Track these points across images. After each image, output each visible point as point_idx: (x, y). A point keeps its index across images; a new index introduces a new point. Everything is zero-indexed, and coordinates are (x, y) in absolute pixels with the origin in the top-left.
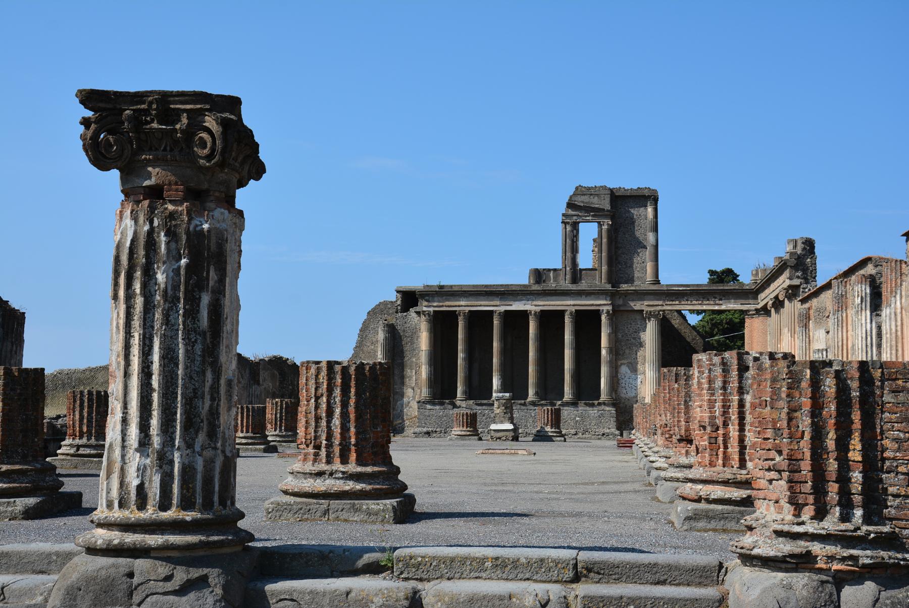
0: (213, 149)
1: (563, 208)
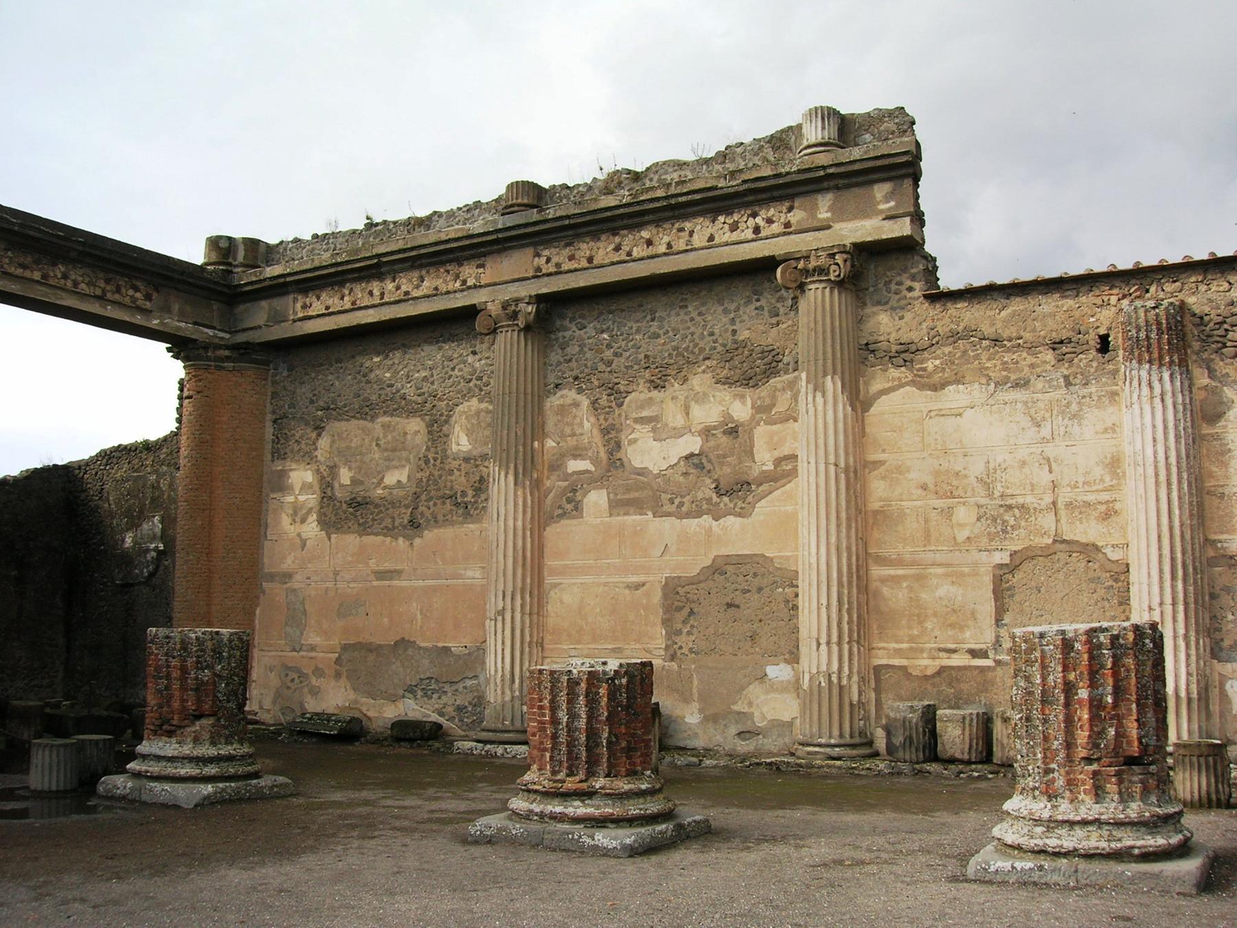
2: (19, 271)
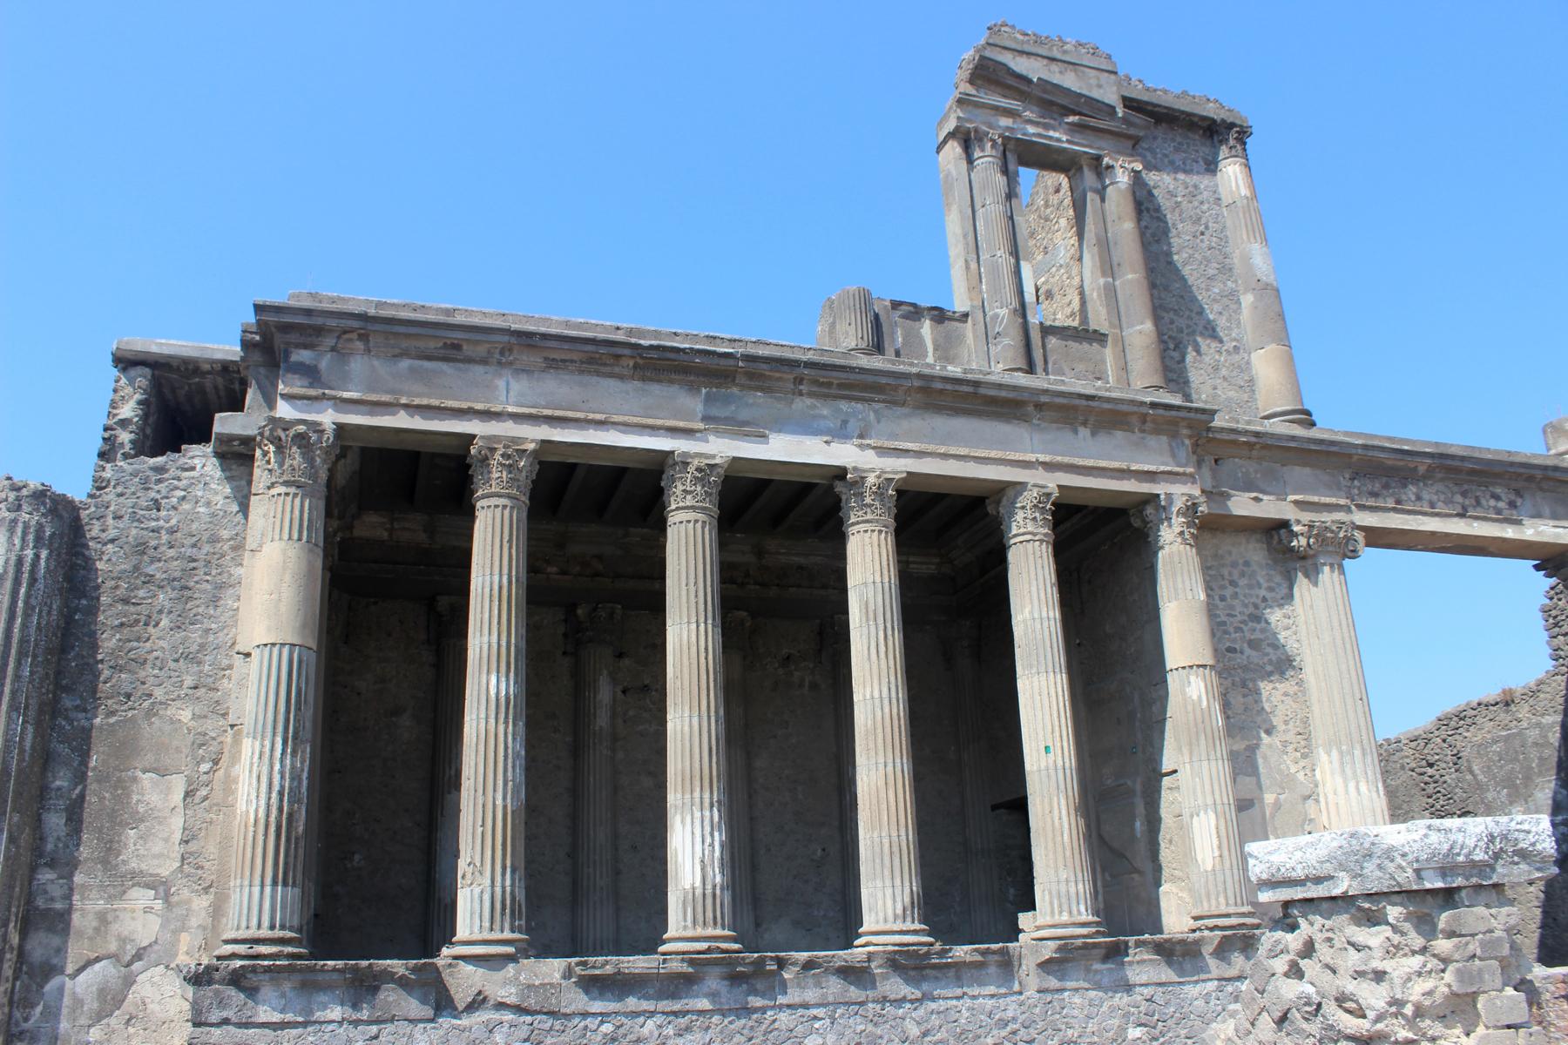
1: (957, 81)
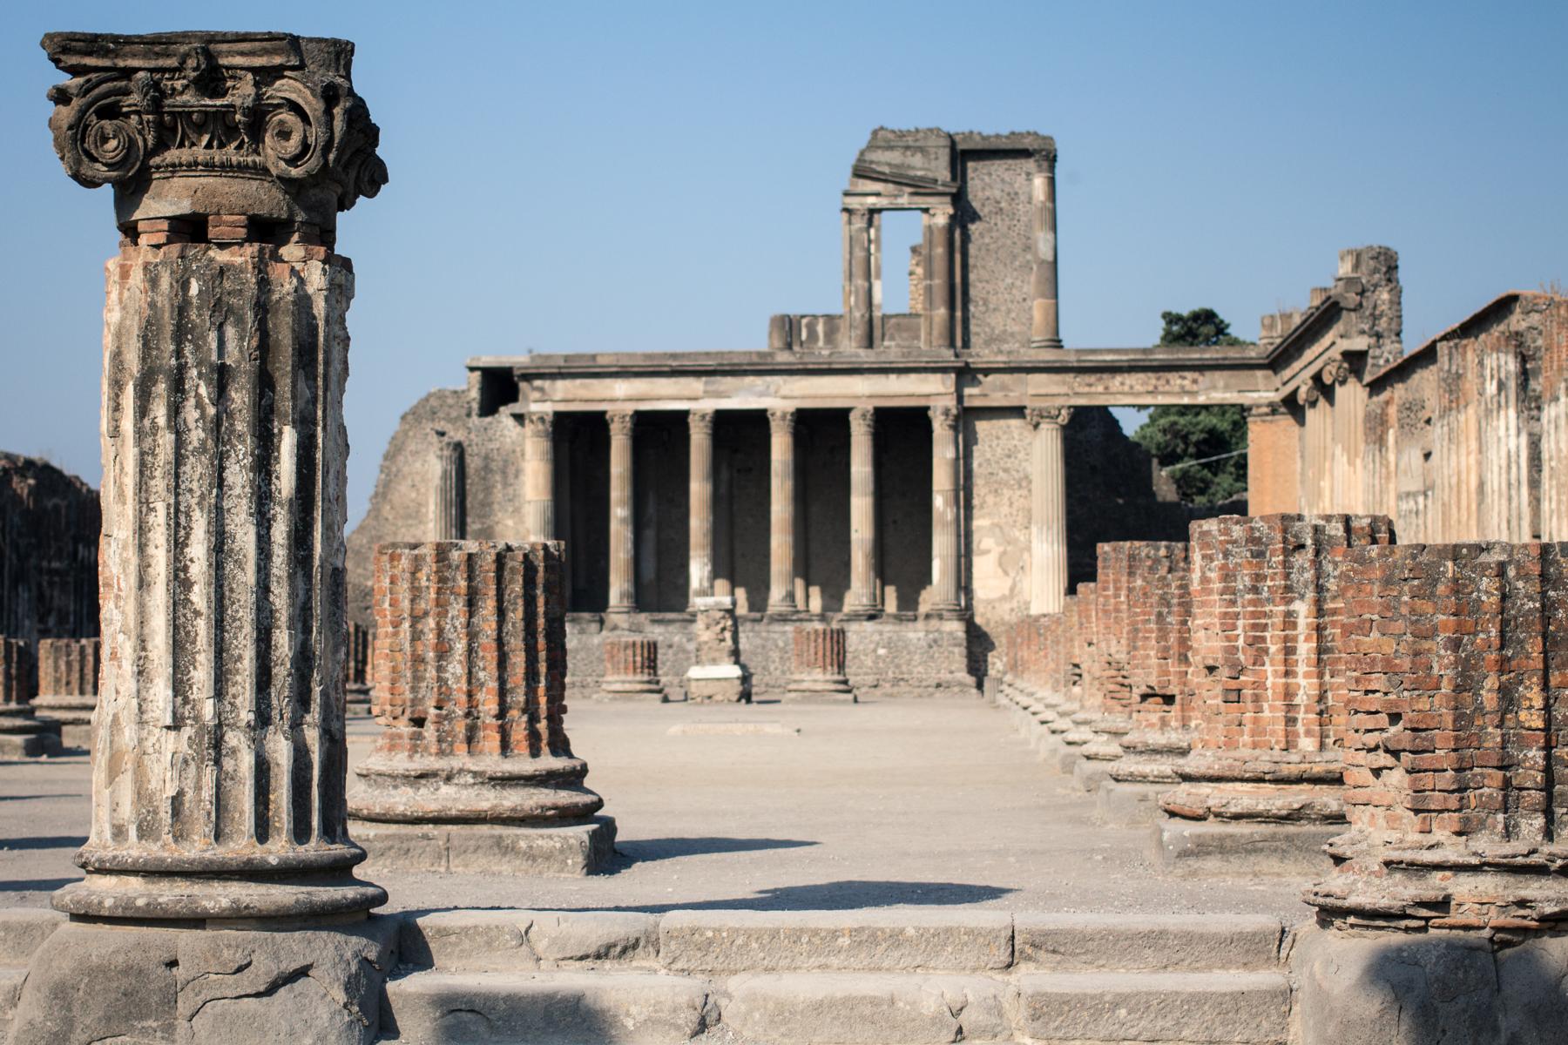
0: (305, 147)
1: (845, 179)
2: (1086, 389)
